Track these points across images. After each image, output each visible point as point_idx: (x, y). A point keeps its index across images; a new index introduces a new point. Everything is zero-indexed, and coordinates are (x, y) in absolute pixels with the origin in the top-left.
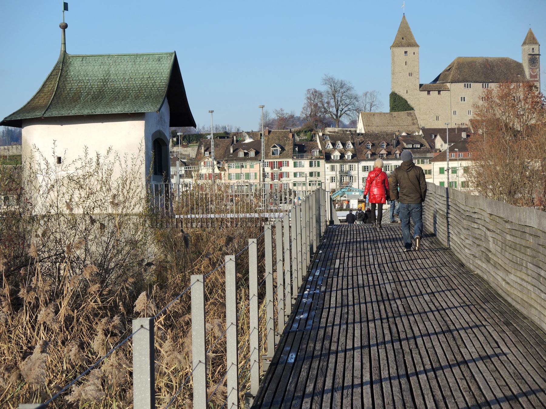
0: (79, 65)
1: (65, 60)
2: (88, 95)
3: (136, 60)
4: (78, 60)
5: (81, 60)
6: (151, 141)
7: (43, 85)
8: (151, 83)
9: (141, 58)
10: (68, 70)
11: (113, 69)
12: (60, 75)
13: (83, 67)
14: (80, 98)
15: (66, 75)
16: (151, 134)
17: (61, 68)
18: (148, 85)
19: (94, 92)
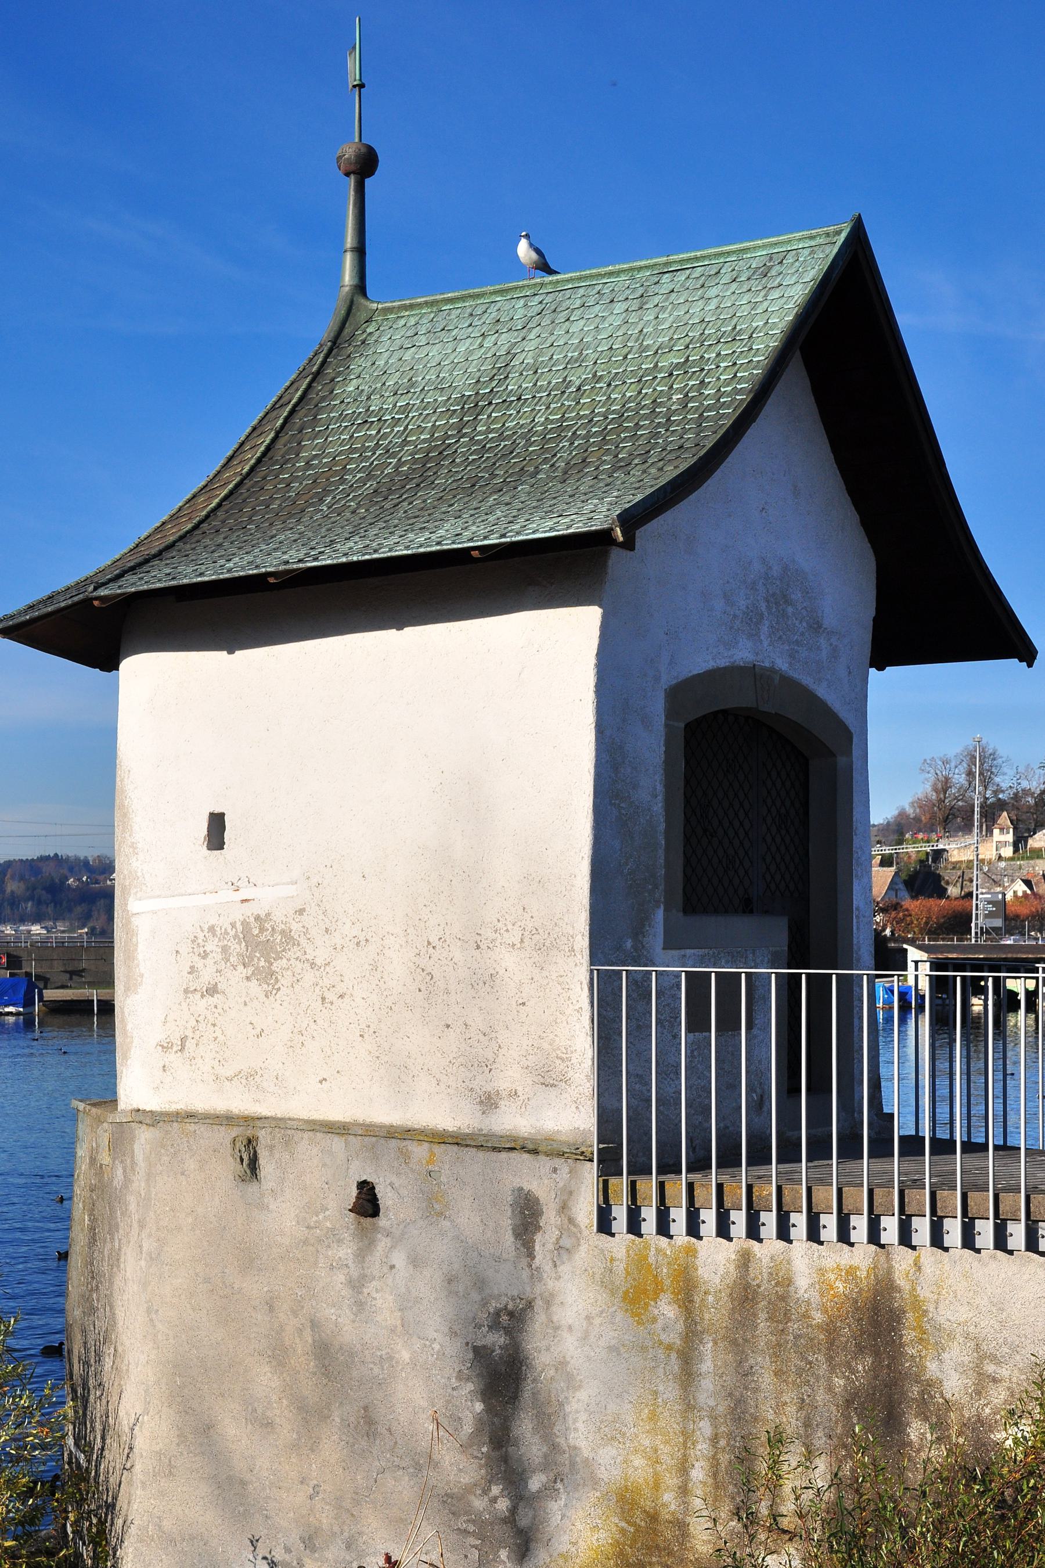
0: (398, 343)
1: (347, 331)
2: (370, 476)
3: (652, 290)
4: (402, 322)
5: (412, 321)
6: (659, 720)
7: (230, 459)
8: (680, 391)
9: (682, 277)
10: (339, 374)
11: (532, 346)
12: (301, 399)
13: (408, 356)
14: (321, 500)
15: (323, 399)
16: (667, 680)
17: (315, 369)
18: (660, 405)
19: (400, 463)
